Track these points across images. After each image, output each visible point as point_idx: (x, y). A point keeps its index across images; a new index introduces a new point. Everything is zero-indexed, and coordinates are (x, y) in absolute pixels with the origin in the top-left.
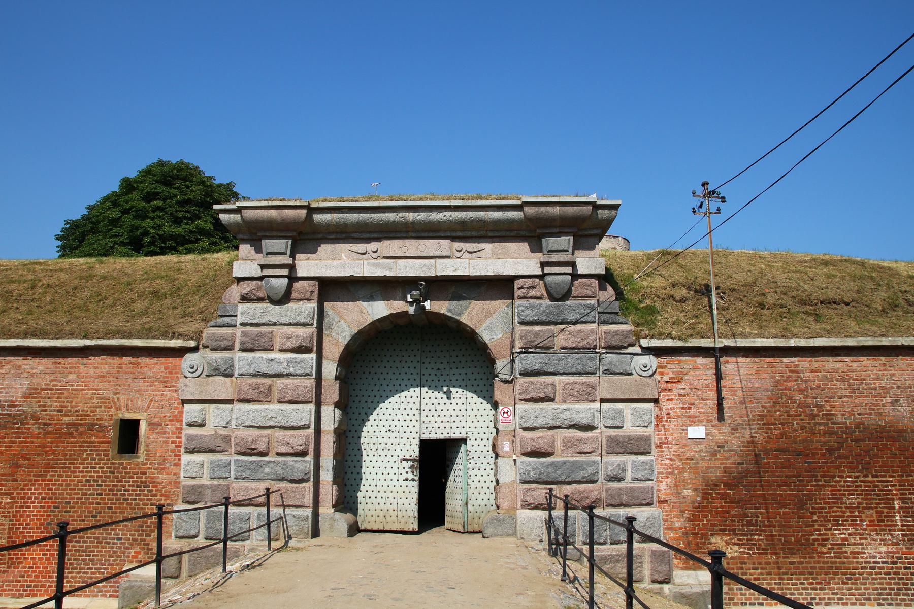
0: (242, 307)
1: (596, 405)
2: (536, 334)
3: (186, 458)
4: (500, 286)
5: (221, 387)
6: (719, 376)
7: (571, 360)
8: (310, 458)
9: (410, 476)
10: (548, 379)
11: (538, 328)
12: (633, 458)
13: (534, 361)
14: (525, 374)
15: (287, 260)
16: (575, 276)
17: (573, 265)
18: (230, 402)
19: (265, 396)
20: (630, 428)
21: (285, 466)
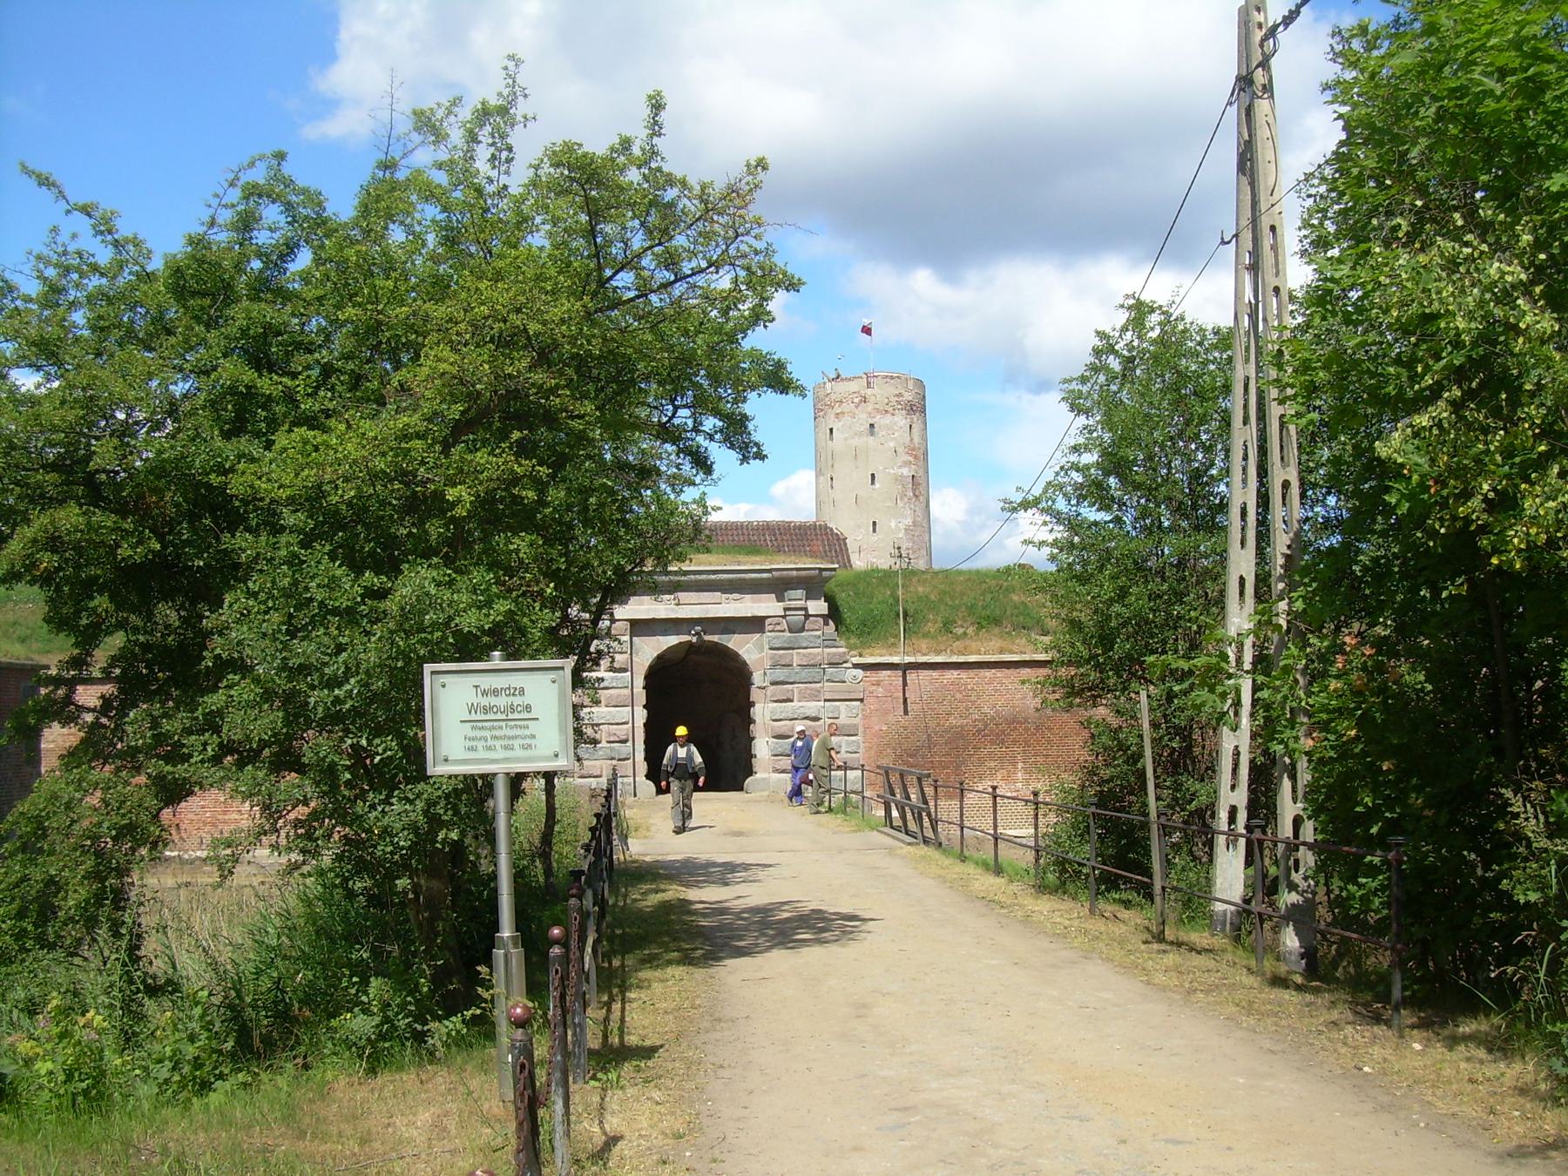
2: (781, 656)
4: (755, 624)
6: (905, 684)
7: (805, 674)
8: (630, 744)
13: (780, 674)
14: (773, 683)
16: (807, 616)
17: (806, 609)
20: (843, 720)
21: (612, 749)
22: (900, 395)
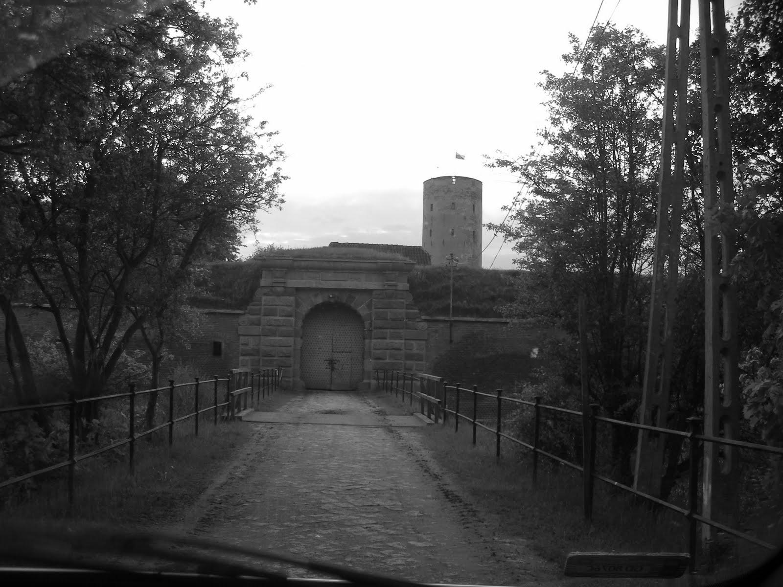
0: (264, 298)
1: (403, 341)
3: (241, 358)
5: (256, 330)
9: (328, 367)
10: (385, 331)
11: (381, 310)
12: (416, 362)
15: (282, 280)
18: (260, 335)
19: (274, 334)
20: (415, 350)
22: (469, 188)
